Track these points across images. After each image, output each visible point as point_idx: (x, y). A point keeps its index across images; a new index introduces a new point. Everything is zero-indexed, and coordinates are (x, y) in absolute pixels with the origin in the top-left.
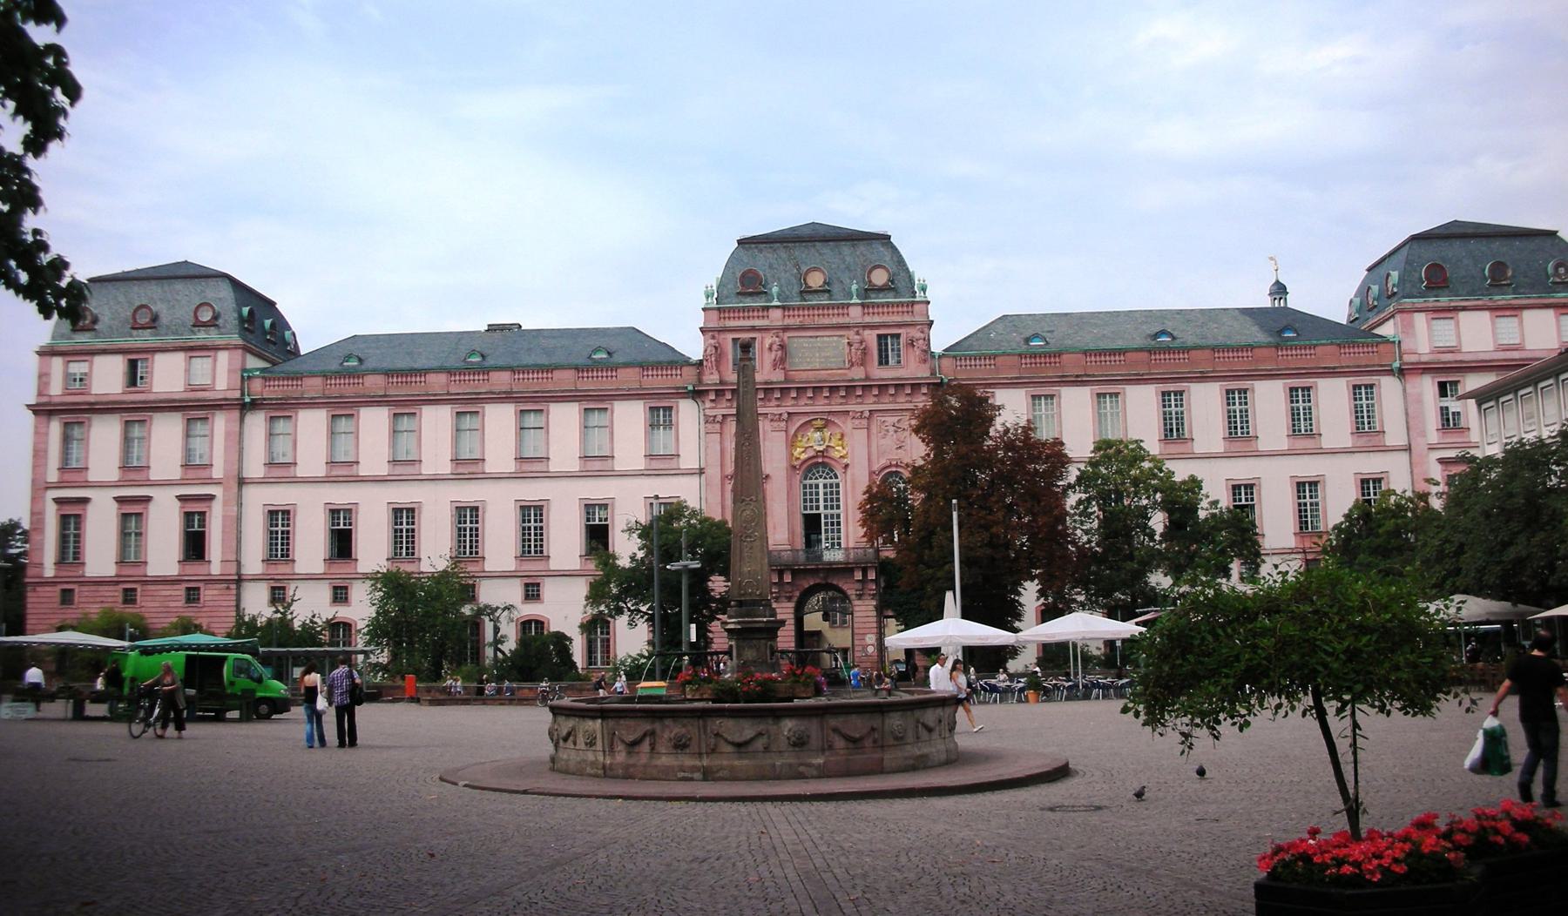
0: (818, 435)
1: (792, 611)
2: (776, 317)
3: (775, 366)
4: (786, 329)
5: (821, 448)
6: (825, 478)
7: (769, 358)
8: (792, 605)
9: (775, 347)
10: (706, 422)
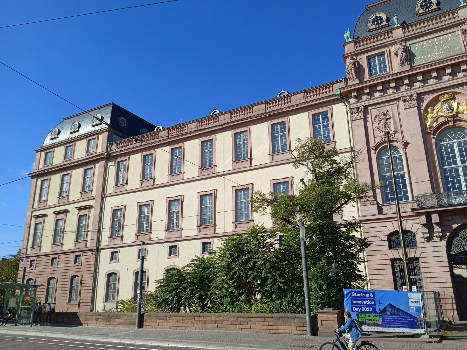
0: (445, 107)
1: (444, 248)
2: (398, 33)
3: (402, 65)
4: (406, 40)
5: (451, 114)
6: (458, 138)
7: (396, 61)
8: (444, 243)
9: (400, 52)
10: (352, 113)
